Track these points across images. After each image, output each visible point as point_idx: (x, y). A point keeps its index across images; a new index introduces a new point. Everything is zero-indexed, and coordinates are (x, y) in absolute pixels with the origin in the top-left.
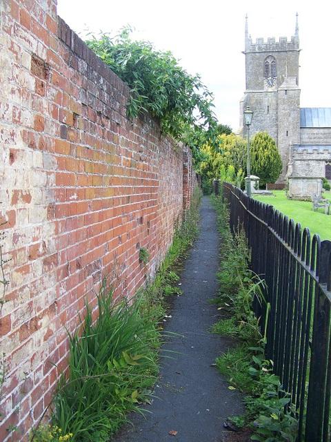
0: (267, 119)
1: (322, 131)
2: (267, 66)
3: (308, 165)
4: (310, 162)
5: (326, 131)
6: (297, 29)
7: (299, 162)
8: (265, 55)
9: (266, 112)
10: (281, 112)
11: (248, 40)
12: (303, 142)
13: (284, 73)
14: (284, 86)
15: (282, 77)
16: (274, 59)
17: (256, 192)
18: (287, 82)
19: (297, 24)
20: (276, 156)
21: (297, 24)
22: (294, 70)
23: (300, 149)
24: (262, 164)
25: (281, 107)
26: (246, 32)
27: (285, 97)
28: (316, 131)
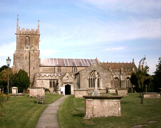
1: (48, 67)
3: (42, 81)
5: (50, 67)
6: (39, 26)
7: (38, 80)
8: (25, 36)
9: (25, 59)
10: (31, 59)
11: (18, 29)
15: (32, 45)
16: (29, 37)
18: (34, 47)
22: (37, 42)
25: (31, 57)
27: (33, 53)
28: (46, 68)
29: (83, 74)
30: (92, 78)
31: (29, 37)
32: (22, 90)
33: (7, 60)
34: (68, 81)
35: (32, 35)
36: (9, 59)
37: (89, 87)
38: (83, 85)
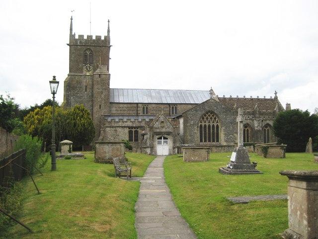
0: (85, 95)
1: (125, 105)
2: (86, 56)
3: (116, 130)
4: (117, 129)
5: (129, 105)
6: (109, 31)
8: (85, 48)
10: (96, 90)
11: (72, 36)
12: (112, 114)
13: (99, 62)
14: (98, 71)
16: (92, 51)
17: (69, 154)
19: (109, 28)
20: (90, 124)
21: (109, 28)
22: (106, 60)
23: (109, 119)
24: (79, 130)
25: (96, 87)
26: (71, 29)
27: (99, 79)
28: (121, 106)
30: (205, 126)
31: (93, 50)
32: (79, 146)
33: (50, 82)
34: (164, 130)
35: (98, 47)
36: (54, 81)
37: (201, 141)
38: (189, 138)
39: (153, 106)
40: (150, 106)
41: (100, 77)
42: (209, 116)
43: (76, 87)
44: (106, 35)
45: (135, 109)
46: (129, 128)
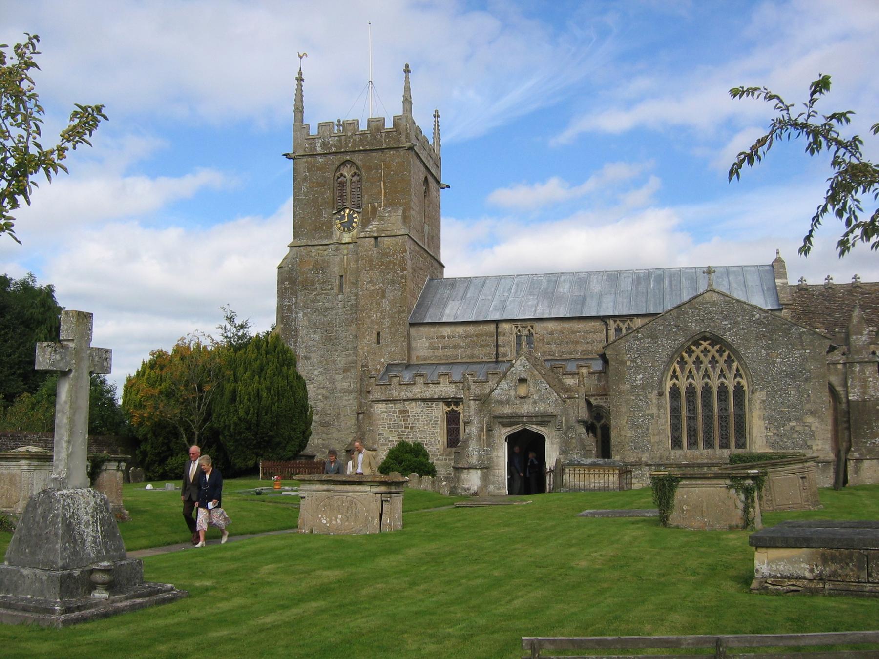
1: (460, 330)
3: (404, 412)
4: (409, 406)
5: (471, 329)
6: (407, 101)
8: (336, 160)
9: (336, 290)
13: (378, 199)
14: (373, 227)
15: (373, 208)
16: (357, 168)
18: (382, 218)
19: (407, 89)
21: (407, 89)
24: (241, 413)
28: (447, 331)
29: (633, 361)
31: (359, 163)
32: (251, 463)
34: (527, 408)
35: (374, 154)
37: (677, 443)
38: (629, 433)
39: (551, 325)
40: (538, 327)
41: (376, 245)
42: (705, 351)
43: (313, 283)
44: (400, 112)
45: (491, 340)
46: (447, 402)
